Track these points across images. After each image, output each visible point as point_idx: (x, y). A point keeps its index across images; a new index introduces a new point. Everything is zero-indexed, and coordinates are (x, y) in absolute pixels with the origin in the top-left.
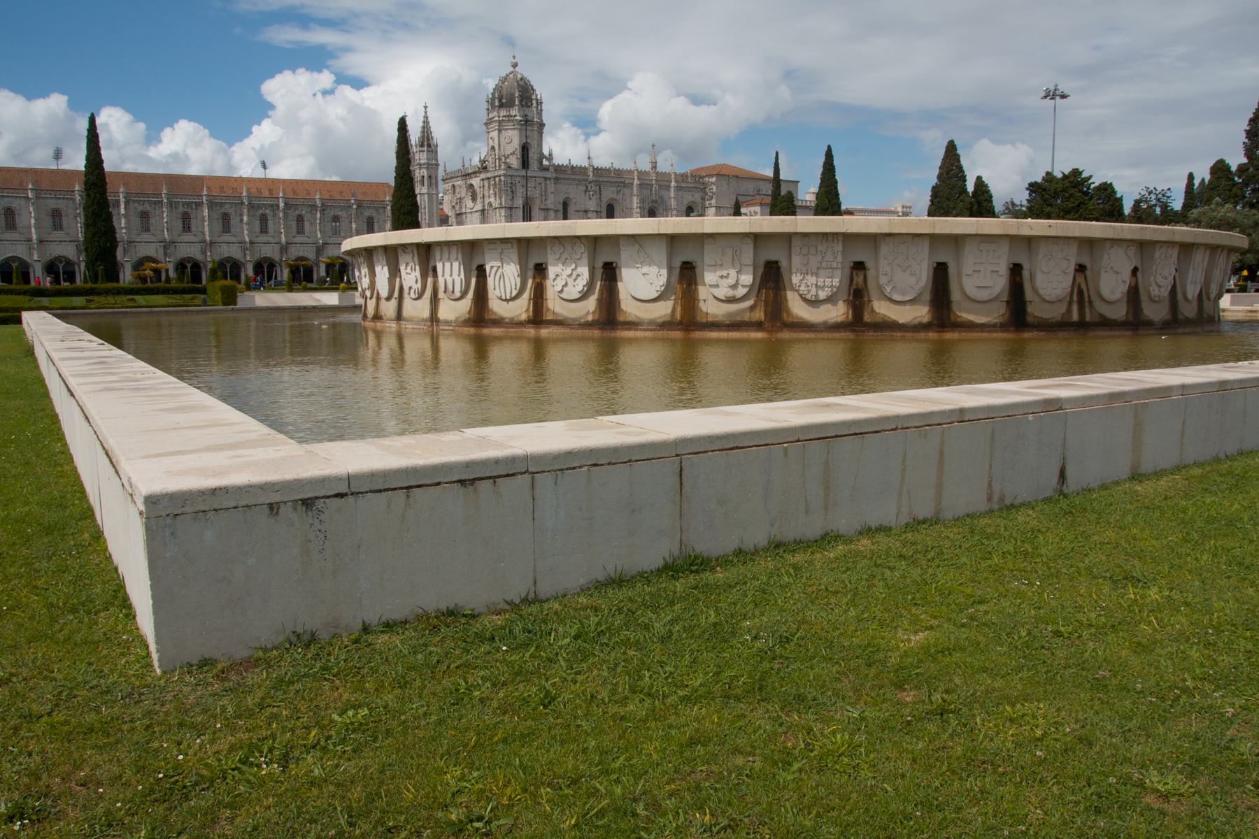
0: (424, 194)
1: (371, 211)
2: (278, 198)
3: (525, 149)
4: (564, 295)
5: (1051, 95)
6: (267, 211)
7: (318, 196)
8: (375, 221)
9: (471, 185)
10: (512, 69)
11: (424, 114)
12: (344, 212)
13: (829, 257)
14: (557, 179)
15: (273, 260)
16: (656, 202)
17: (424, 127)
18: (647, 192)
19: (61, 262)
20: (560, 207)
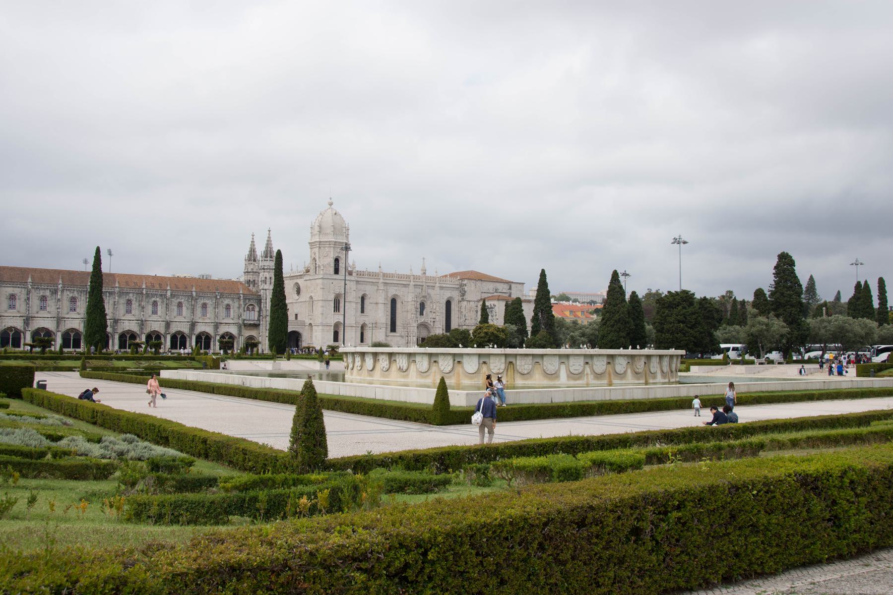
0: (266, 290)
1: (228, 300)
2: (167, 290)
3: (337, 260)
4: (444, 371)
5: (677, 241)
6: (158, 299)
7: (194, 289)
8: (231, 307)
9: (297, 283)
10: (329, 206)
11: (268, 235)
12: (210, 300)
13: (528, 360)
14: (357, 282)
15: (159, 332)
16: (425, 297)
17: (267, 244)
18: (419, 290)
19: (12, 331)
20: (360, 301)
